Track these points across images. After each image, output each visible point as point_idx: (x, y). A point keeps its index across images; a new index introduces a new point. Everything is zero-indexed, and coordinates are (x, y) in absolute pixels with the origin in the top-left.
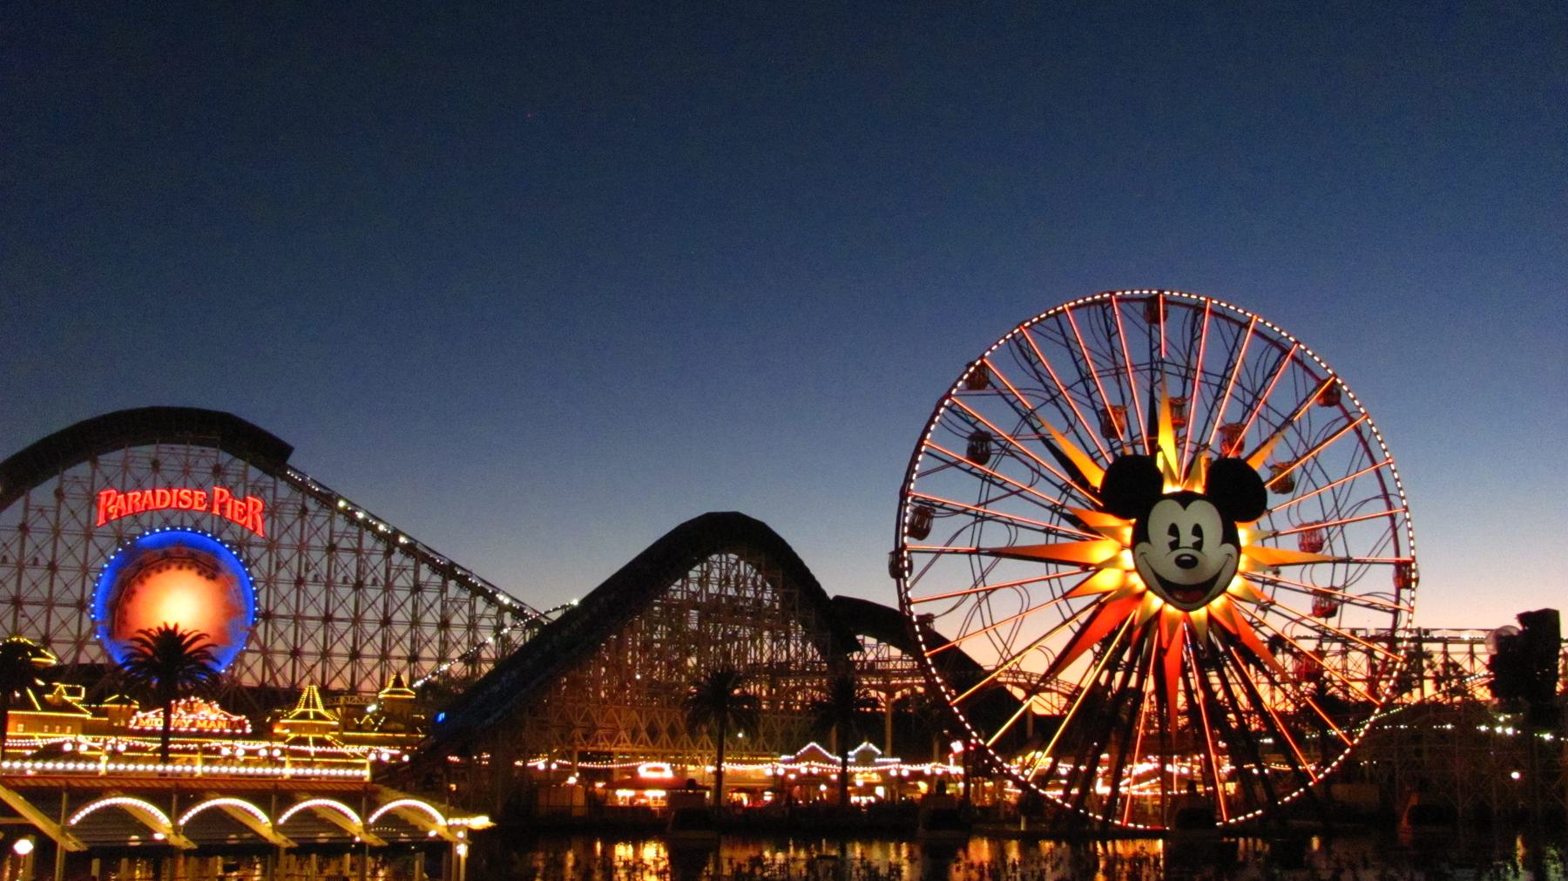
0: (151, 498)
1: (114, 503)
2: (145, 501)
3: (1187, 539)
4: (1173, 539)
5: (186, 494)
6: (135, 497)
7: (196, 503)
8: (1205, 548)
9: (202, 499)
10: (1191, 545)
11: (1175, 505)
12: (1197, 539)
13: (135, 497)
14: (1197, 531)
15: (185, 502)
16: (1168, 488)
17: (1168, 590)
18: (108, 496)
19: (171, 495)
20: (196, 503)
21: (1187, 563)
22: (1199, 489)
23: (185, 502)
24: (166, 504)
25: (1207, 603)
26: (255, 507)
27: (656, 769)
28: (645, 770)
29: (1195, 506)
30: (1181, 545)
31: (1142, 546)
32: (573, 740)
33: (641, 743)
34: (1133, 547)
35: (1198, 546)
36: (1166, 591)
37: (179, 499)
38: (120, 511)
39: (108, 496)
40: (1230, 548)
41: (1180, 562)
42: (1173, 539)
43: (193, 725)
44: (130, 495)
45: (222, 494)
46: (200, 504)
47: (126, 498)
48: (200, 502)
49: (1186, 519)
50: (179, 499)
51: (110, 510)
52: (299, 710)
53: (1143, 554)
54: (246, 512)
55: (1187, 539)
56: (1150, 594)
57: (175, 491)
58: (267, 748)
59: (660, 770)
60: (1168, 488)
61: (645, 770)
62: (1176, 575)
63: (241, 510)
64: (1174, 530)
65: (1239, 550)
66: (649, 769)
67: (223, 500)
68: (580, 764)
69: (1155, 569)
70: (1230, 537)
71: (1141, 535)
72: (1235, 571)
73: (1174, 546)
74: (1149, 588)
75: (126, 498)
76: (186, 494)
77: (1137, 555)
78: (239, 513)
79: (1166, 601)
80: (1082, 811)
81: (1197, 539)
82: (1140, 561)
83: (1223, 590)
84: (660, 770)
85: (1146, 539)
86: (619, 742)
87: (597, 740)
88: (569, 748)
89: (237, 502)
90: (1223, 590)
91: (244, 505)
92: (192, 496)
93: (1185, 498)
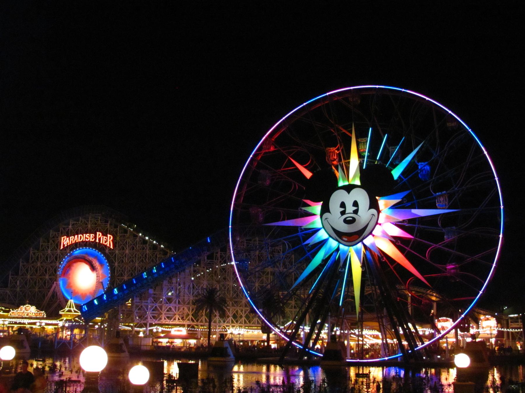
0: (77, 238)
1: (66, 241)
2: (75, 240)
3: (350, 209)
4: (343, 209)
5: (88, 236)
6: (72, 238)
7: (91, 238)
8: (359, 213)
9: (93, 237)
10: (352, 212)
11: (344, 192)
12: (355, 208)
13: (72, 238)
14: (355, 204)
15: (87, 239)
16: (341, 183)
17: (339, 235)
18: (64, 239)
19: (83, 236)
20: (91, 238)
21: (349, 222)
22: (358, 182)
23: (87, 239)
24: (81, 240)
25: (362, 241)
26: (110, 237)
27: (178, 331)
28: (174, 331)
29: (354, 191)
30: (346, 213)
31: (326, 215)
32: (147, 318)
33: (189, 320)
34: (321, 216)
35: (356, 212)
36: (338, 236)
37: (86, 238)
38: (67, 244)
39: (64, 239)
40: (374, 211)
41: (346, 221)
42: (343, 209)
43: (27, 315)
44: (71, 237)
45: (99, 235)
46: (92, 239)
47: (69, 239)
48: (92, 238)
49: (349, 199)
50: (86, 238)
51: (65, 244)
52: (67, 309)
53: (326, 219)
54: (107, 240)
55: (350, 209)
56: (331, 239)
57: (84, 235)
58: (40, 322)
59: (181, 331)
60: (341, 183)
61: (174, 331)
62: (344, 228)
63: (106, 240)
64: (343, 205)
65: (379, 212)
66: (175, 331)
67: (100, 237)
68: (149, 329)
69: (333, 227)
70: (374, 205)
71: (325, 209)
72: (377, 223)
73: (343, 213)
74: (330, 236)
75: (69, 239)
76: (88, 236)
77: (323, 220)
78: (105, 241)
79: (339, 242)
80: (307, 350)
81: (355, 208)
82: (325, 223)
83: (371, 233)
84: (181, 331)
85: (329, 211)
86: (175, 319)
87: (161, 319)
88: (145, 322)
89: (104, 237)
90: (371, 233)
91: (106, 238)
92: (90, 236)
93: (349, 188)
